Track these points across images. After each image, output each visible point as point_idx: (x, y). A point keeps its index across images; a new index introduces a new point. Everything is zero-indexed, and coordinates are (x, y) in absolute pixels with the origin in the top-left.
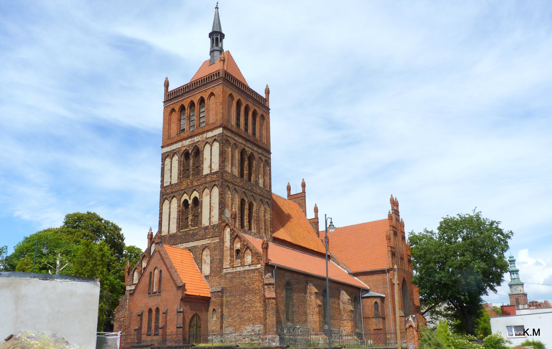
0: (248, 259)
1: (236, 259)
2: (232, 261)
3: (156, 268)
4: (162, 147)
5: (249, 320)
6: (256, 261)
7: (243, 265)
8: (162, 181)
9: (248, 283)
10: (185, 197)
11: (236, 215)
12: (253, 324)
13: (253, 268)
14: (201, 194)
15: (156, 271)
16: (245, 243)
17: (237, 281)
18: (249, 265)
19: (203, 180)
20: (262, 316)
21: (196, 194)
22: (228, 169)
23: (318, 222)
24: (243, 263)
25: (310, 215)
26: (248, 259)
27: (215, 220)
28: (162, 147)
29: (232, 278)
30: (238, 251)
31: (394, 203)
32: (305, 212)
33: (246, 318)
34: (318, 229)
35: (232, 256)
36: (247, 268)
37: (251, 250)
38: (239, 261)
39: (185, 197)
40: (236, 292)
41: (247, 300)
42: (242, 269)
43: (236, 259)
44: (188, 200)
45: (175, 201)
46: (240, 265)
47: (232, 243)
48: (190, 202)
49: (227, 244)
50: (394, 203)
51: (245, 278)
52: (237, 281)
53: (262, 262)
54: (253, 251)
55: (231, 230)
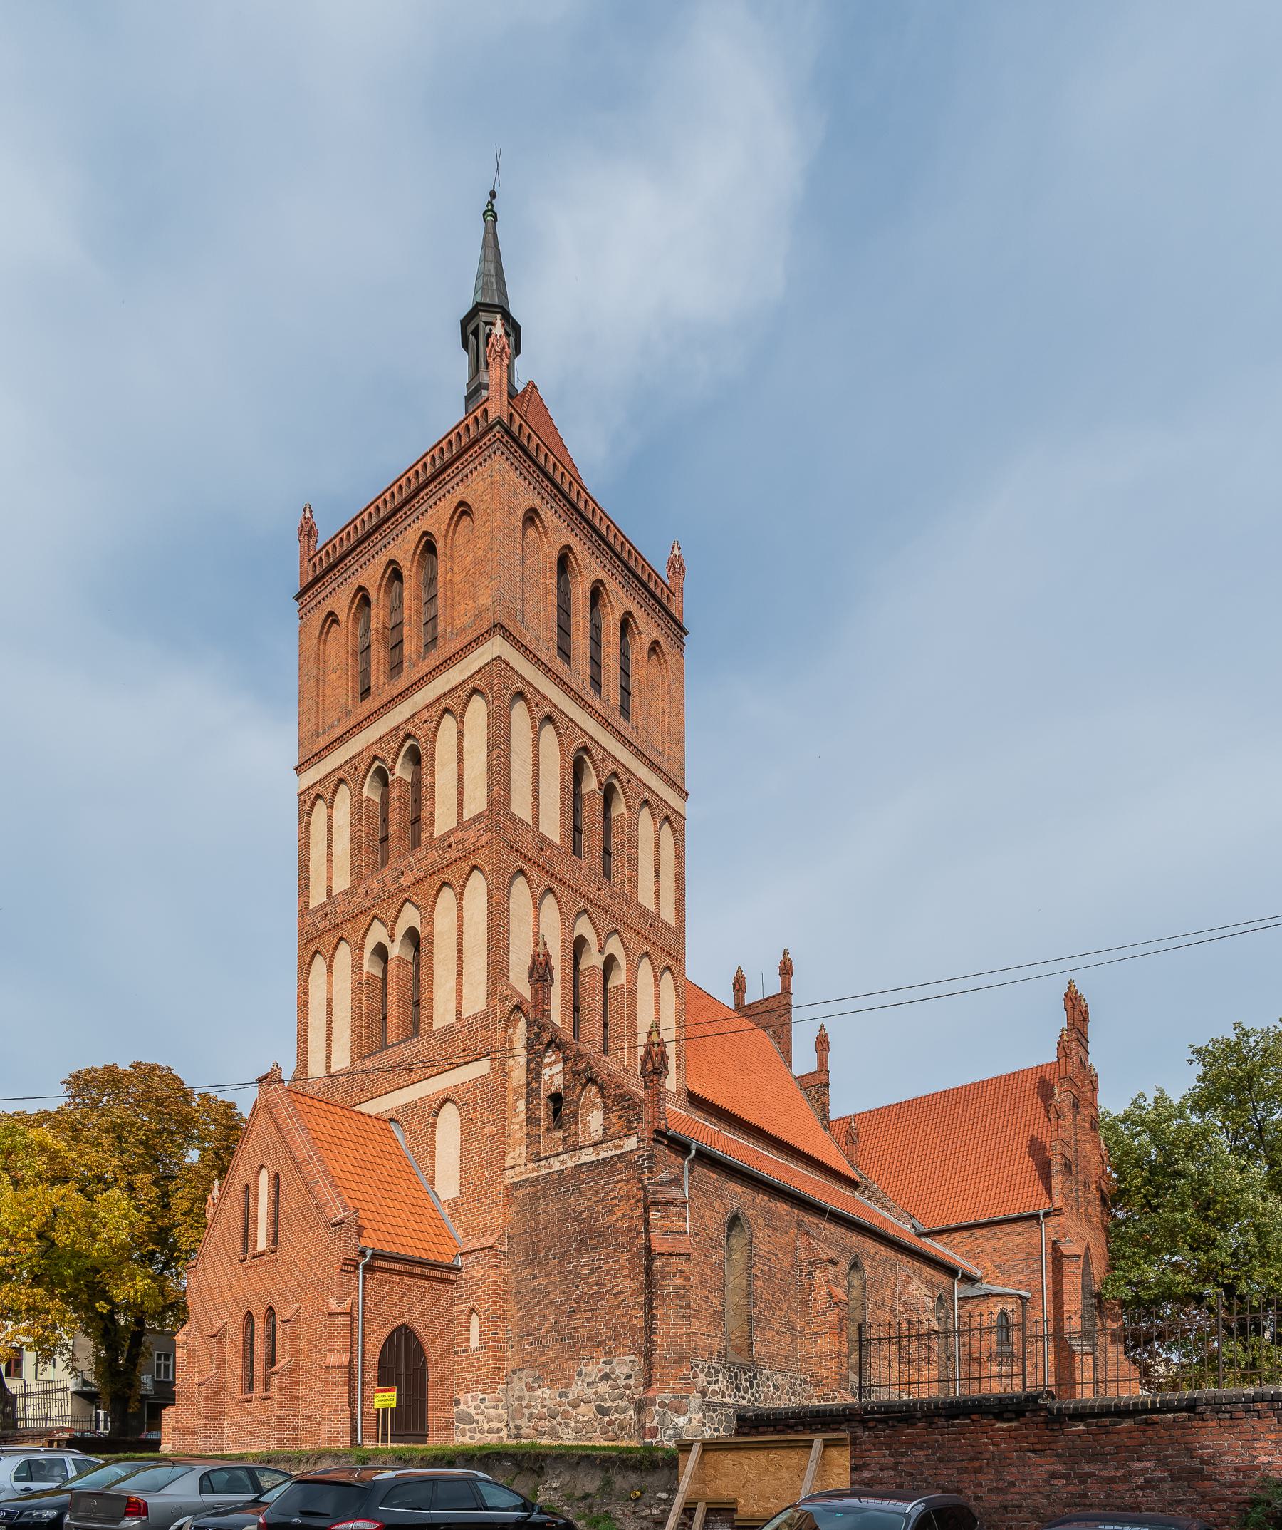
0: (595, 1121)
1: (549, 1130)
2: (532, 1140)
3: (262, 1166)
4: (300, 769)
5: (593, 1341)
6: (618, 1126)
7: (571, 1147)
10: (378, 933)
12: (608, 1353)
13: (610, 1154)
14: (428, 912)
15: (264, 1178)
16: (582, 1066)
18: (596, 1144)
20: (640, 1323)
22: (521, 807)
23: (827, 1085)
25: (804, 1062)
26: (595, 1121)
27: (476, 1002)
28: (300, 769)
29: (535, 1197)
30: (556, 1098)
31: (1075, 1005)
32: (786, 1054)
33: (583, 1333)
34: (824, 1107)
35: (532, 1121)
36: (587, 1156)
38: (560, 1134)
39: (378, 933)
40: (547, 1248)
41: (585, 1270)
42: (569, 1162)
43: (549, 1130)
45: (344, 954)
46: (561, 1149)
47: (534, 1073)
48: (395, 950)
49: (519, 1075)
50: (1075, 1005)
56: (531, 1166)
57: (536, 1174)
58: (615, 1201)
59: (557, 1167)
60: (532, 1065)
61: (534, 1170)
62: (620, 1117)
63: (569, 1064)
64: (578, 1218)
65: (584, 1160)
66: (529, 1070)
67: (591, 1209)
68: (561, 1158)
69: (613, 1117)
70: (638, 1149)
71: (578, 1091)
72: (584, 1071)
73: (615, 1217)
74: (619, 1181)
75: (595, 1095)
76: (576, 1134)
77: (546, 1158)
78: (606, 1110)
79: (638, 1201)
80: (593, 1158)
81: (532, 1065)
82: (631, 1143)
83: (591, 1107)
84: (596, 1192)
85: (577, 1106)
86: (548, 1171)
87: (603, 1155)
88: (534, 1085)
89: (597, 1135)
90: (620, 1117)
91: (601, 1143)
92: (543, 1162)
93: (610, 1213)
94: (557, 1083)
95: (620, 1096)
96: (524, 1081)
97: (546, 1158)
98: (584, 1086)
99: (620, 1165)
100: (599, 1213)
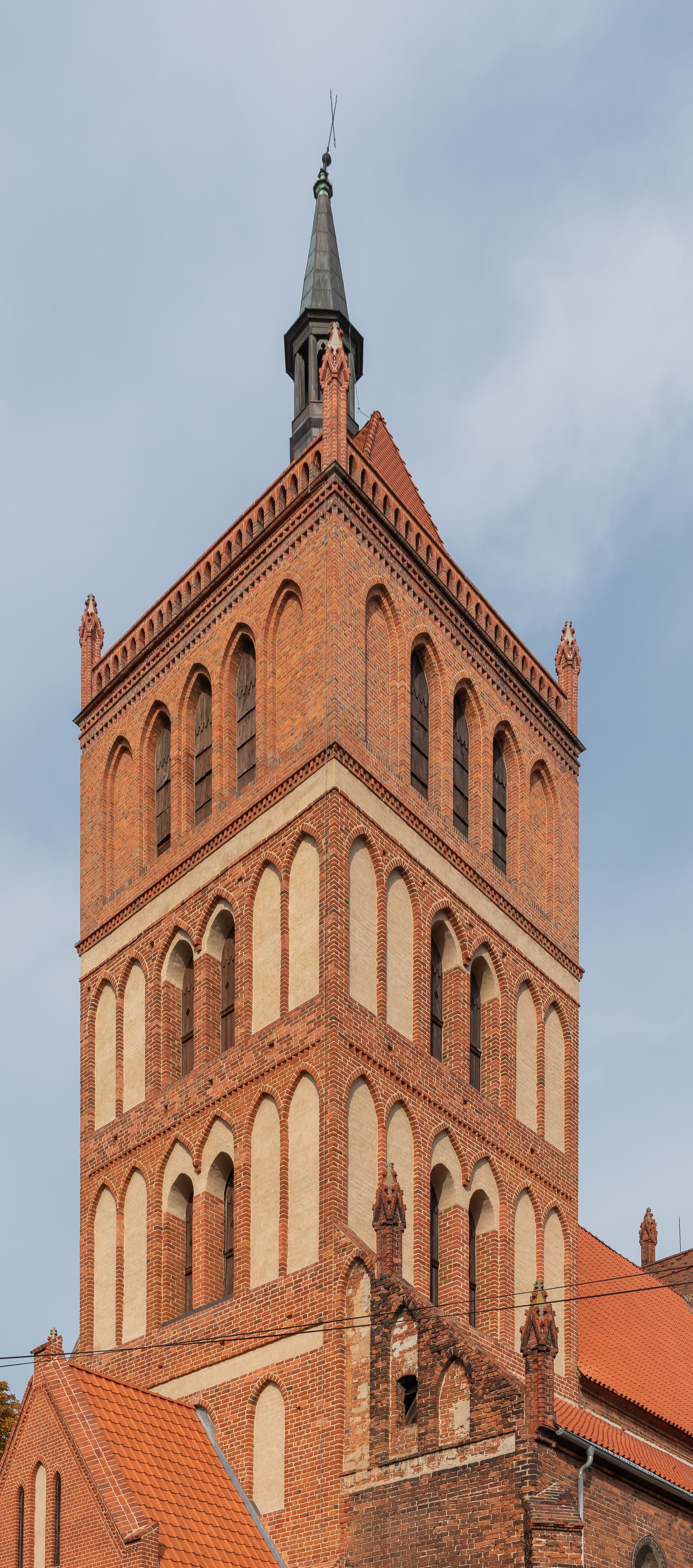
0: (458, 1415)
1: (399, 1424)
2: (378, 1438)
7: (430, 1450)
8: (88, 1104)
9: (454, 1532)
11: (399, 1206)
13: (479, 1458)
16: (443, 1340)
17: (403, 1527)
18: (461, 1445)
19: (249, 1063)
21: (221, 1140)
24: (429, 1438)
26: (458, 1415)
29: (381, 1513)
30: (409, 1383)
35: (377, 1412)
36: (449, 1460)
37: (468, 1371)
38: (413, 1430)
43: (399, 1424)
44: (191, 1173)
45: (138, 1186)
46: (415, 1450)
47: (380, 1348)
51: (440, 1508)
52: (403, 1527)
53: (522, 1423)
54: (482, 1373)
55: (374, 1284)
56: (376, 1471)
57: (382, 1483)
58: (487, 1522)
59: (410, 1474)
60: (378, 1338)
61: (380, 1478)
62: (494, 1409)
63: (426, 1337)
64: (437, 1542)
65: (446, 1465)
66: (373, 1344)
67: (454, 1532)
68: (415, 1462)
69: (485, 1408)
70: (516, 1453)
71: (438, 1373)
72: (446, 1347)
73: (486, 1543)
74: (492, 1495)
75: (459, 1378)
76: (435, 1431)
77: (396, 1462)
78: (475, 1399)
79: (516, 1523)
80: (457, 1463)
81: (378, 1338)
82: (508, 1445)
83: (454, 1394)
84: (461, 1509)
85: (436, 1393)
86: (398, 1479)
87: (471, 1459)
88: (380, 1365)
89: (462, 1433)
90: (494, 1409)
91: (469, 1443)
92: (392, 1467)
93: (480, 1537)
94: (410, 1362)
95: (494, 1380)
96: (366, 1358)
97: (396, 1462)
98: (446, 1367)
99: (493, 1474)
100: (465, 1537)
